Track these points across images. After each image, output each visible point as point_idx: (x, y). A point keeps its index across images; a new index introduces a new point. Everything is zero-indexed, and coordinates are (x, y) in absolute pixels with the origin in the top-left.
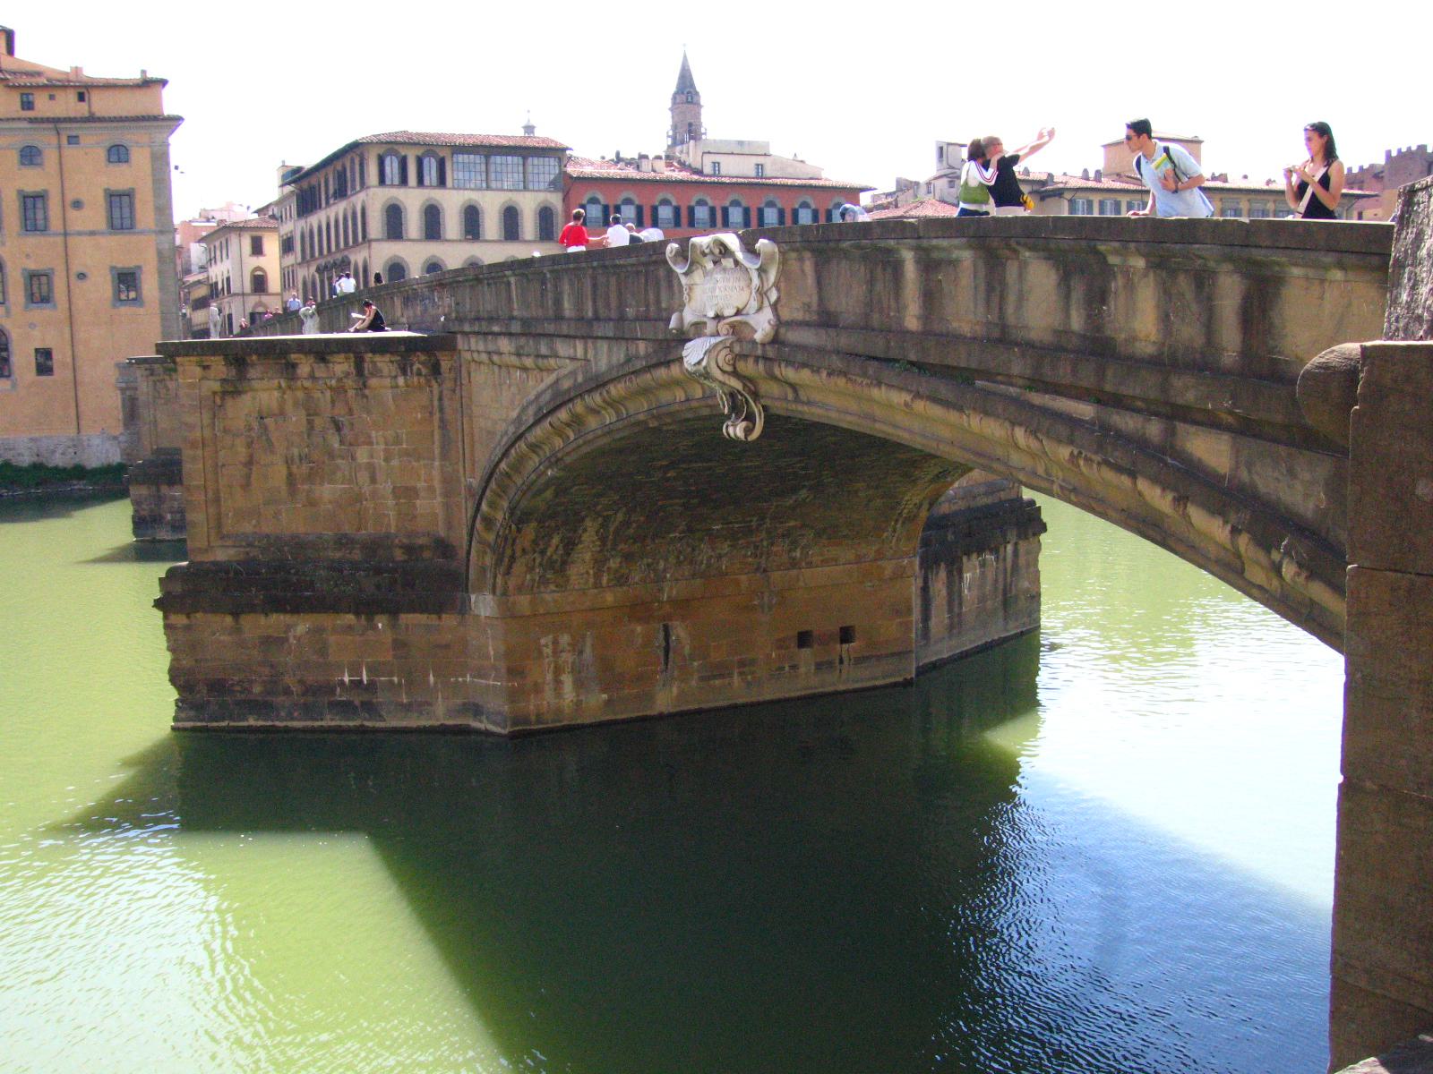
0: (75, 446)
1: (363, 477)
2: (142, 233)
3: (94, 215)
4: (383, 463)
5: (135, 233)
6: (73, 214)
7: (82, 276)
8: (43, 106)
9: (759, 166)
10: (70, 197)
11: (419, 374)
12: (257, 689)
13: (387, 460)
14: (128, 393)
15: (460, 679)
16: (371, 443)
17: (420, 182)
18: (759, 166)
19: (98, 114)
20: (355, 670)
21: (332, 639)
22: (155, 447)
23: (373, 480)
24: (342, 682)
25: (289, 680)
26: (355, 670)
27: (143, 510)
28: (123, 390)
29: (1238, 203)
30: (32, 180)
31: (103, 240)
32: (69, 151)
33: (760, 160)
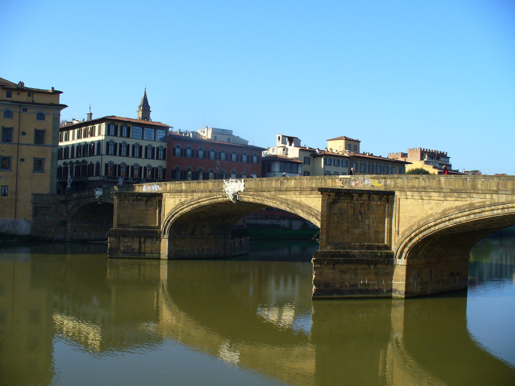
0: (13, 224)
1: (366, 228)
2: (47, 146)
3: (30, 138)
4: (372, 224)
5: (44, 146)
6: (22, 137)
7: (22, 160)
8: (15, 97)
9: (229, 139)
10: (22, 130)
11: (384, 201)
13: (373, 223)
14: (35, 205)
16: (369, 219)
17: (121, 136)
18: (229, 139)
19: (35, 102)
21: (359, 271)
22: (118, 224)
23: (369, 229)
26: (364, 280)
27: (113, 245)
28: (33, 204)
29: (373, 163)
30: (8, 123)
31: (32, 147)
32: (24, 114)
33: (229, 137)
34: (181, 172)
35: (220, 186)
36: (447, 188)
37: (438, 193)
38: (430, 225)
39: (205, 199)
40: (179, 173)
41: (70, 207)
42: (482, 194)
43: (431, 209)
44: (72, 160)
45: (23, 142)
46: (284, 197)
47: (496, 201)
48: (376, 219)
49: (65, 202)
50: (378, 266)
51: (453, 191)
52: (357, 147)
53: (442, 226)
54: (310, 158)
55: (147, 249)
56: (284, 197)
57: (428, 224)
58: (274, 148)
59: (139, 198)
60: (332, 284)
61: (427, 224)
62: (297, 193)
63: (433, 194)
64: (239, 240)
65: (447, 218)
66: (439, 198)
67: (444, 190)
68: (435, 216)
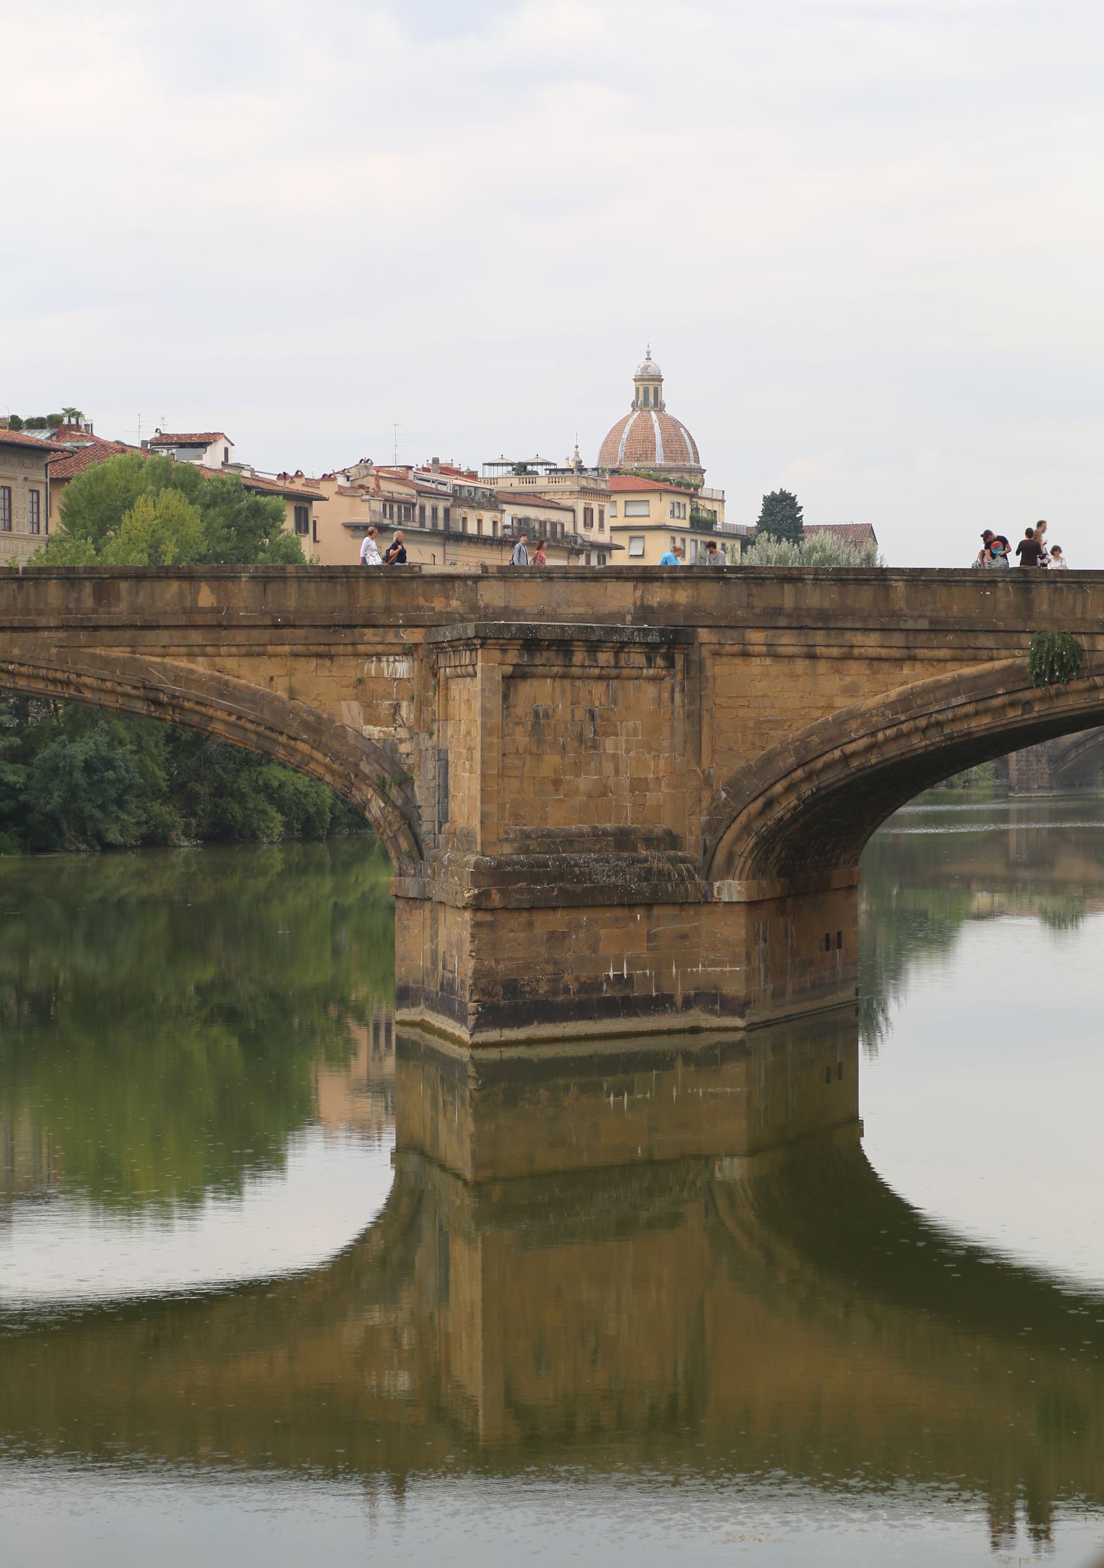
1: (608, 768)
12: (543, 988)
13: (627, 751)
15: (694, 969)
16: (616, 735)
23: (617, 772)
24: (608, 976)
36: (916, 613)
37: (880, 633)
38: (850, 748)
42: (969, 633)
46: (117, 653)
50: (656, 911)
51: (938, 628)
53: (892, 751)
56: (117, 653)
57: (846, 744)
60: (528, 984)
61: (837, 748)
62: (196, 637)
63: (858, 639)
65: (922, 722)
66: (884, 652)
67: (910, 625)
68: (872, 715)
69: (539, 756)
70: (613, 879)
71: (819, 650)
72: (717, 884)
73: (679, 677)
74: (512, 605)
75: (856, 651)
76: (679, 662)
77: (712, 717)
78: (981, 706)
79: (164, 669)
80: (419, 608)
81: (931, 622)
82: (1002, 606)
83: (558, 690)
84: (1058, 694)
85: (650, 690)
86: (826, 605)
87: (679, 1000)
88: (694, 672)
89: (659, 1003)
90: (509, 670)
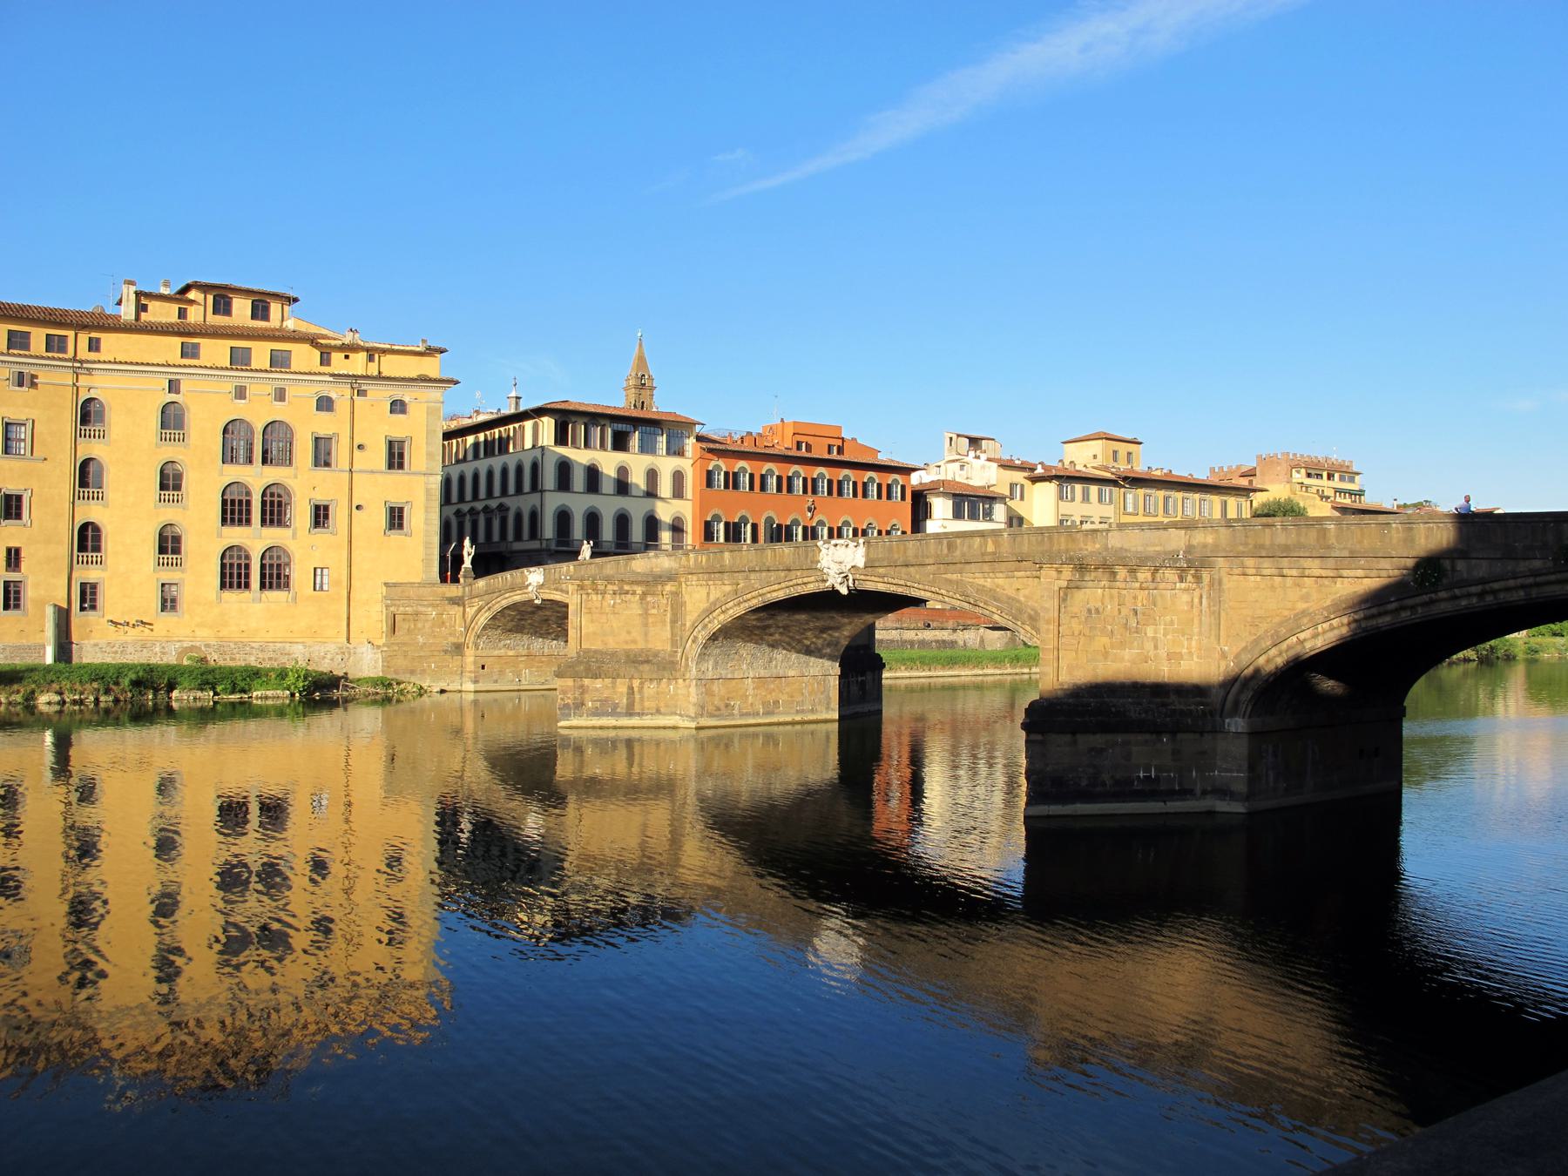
0: (344, 653)
1: (1149, 646)
7: (358, 507)
12: (1084, 783)
13: (1165, 635)
17: (587, 445)
20: (1147, 769)
23: (1156, 647)
25: (1106, 777)
26: (1147, 769)
31: (380, 478)
34: (727, 525)
35: (810, 555)
36: (1342, 546)
39: (776, 587)
40: (722, 526)
41: (470, 611)
43: (1305, 598)
44: (473, 504)
45: (364, 468)
46: (954, 577)
47: (1465, 575)
48: (1172, 623)
49: (457, 601)
50: (1179, 736)
52: (1134, 455)
54: (1022, 486)
55: (647, 704)
56: (954, 577)
58: (938, 464)
59: (626, 587)
63: (1307, 563)
64: (860, 679)
66: (1324, 573)
69: (1091, 638)
70: (1144, 715)
71: (1285, 572)
72: (1227, 721)
73: (1206, 588)
74: (1125, 546)
75: (1307, 572)
76: (1206, 576)
77: (1227, 614)
78: (1382, 609)
79: (972, 585)
80: (1081, 550)
81: (1351, 552)
82: (1394, 541)
83: (1107, 597)
84: (1432, 602)
85: (1185, 598)
86: (1289, 542)
87: (1198, 791)
88: (1216, 584)
89: (1185, 793)
90: (1065, 584)
